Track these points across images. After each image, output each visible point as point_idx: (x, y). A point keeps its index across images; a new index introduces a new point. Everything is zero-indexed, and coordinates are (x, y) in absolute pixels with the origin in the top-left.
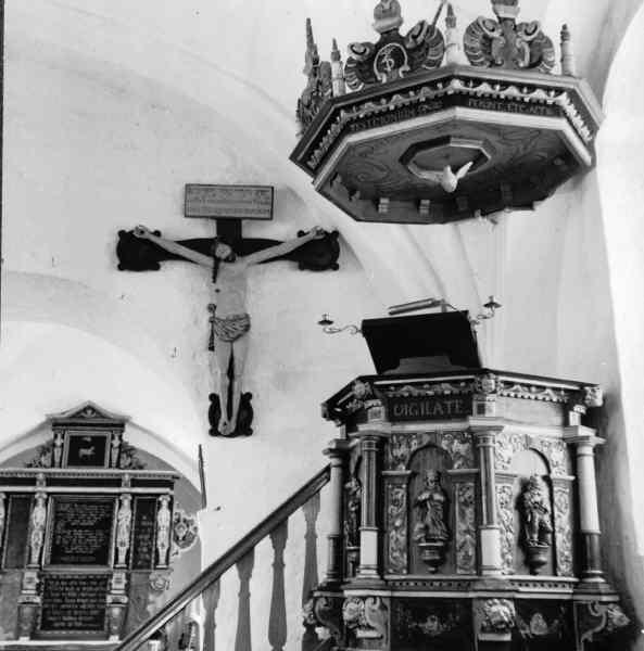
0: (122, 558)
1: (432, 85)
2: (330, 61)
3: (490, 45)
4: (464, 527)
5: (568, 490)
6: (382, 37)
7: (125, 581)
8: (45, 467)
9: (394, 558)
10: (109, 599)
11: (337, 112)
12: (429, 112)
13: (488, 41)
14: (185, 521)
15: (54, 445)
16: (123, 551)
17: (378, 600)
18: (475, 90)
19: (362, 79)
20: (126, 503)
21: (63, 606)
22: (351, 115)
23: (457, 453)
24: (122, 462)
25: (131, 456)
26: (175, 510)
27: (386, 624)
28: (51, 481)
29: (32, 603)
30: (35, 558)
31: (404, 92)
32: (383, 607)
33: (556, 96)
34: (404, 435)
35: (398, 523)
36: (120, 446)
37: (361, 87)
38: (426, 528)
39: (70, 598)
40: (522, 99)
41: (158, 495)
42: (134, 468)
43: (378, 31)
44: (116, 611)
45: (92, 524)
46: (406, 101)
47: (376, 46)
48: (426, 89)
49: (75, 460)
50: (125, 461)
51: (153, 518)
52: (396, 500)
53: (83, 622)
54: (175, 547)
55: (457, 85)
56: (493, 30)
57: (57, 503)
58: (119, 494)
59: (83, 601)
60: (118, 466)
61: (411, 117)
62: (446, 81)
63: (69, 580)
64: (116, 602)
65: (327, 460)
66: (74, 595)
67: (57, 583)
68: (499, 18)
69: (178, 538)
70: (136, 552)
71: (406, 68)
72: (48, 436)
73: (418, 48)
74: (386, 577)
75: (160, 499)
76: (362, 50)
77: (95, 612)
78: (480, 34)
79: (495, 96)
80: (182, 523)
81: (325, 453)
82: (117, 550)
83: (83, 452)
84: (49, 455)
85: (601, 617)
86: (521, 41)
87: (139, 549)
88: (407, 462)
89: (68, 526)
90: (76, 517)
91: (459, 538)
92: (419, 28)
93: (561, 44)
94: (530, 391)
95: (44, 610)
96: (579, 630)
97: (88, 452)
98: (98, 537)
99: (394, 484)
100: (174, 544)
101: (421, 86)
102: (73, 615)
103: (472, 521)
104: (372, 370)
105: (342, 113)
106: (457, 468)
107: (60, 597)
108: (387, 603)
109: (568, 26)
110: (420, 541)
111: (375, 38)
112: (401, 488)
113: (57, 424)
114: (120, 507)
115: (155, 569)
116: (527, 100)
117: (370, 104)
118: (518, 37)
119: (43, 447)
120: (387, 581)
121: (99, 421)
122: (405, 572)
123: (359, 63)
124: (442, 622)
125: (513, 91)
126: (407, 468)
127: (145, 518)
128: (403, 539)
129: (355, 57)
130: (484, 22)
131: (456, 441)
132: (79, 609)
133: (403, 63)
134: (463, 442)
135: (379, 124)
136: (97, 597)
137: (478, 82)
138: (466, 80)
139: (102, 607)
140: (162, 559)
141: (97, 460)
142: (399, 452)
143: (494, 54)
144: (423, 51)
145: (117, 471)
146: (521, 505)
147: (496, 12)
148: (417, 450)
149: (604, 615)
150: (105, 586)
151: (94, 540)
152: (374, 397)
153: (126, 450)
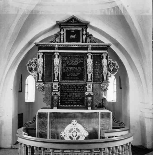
0: (89, 78)
7: (92, 87)
8: (57, 42)
10: (86, 93)
14: (113, 63)
15: (60, 34)
16: (89, 75)
20: (90, 56)
21: (68, 96)
24: (87, 40)
25: (91, 38)
26: (108, 59)
28: (60, 48)
29: (57, 95)
30: (56, 78)
36: (86, 34)
39: (71, 93)
41: (102, 53)
42: (92, 43)
44: (90, 98)
45: (76, 65)
49: (69, 40)
50: (89, 40)
51: (101, 63)
53: (76, 102)
54: (110, 74)
57: (62, 57)
58: (87, 53)
59: (76, 94)
60: (86, 42)
63: (70, 86)
64: (89, 95)
66: (72, 92)
67: (65, 87)
69: (110, 70)
70: (94, 76)
72: (57, 30)
75: (103, 55)
77: (81, 98)
80: (111, 64)
82: (87, 75)
83: (72, 36)
84: (59, 38)
87: (95, 74)
89: (67, 66)
90: (70, 63)
95: (61, 97)
97: (74, 37)
98: (79, 70)
100: (109, 73)
102: (72, 99)
107: (67, 92)
113: (60, 25)
114: (87, 59)
115: (102, 82)
119: (56, 35)
121: (77, 24)
127: (97, 62)
132: (74, 97)
136: (81, 93)
139: (83, 96)
140: (105, 78)
141: (78, 40)
145: (86, 44)
150: (84, 88)
151: (78, 71)
153: (89, 36)
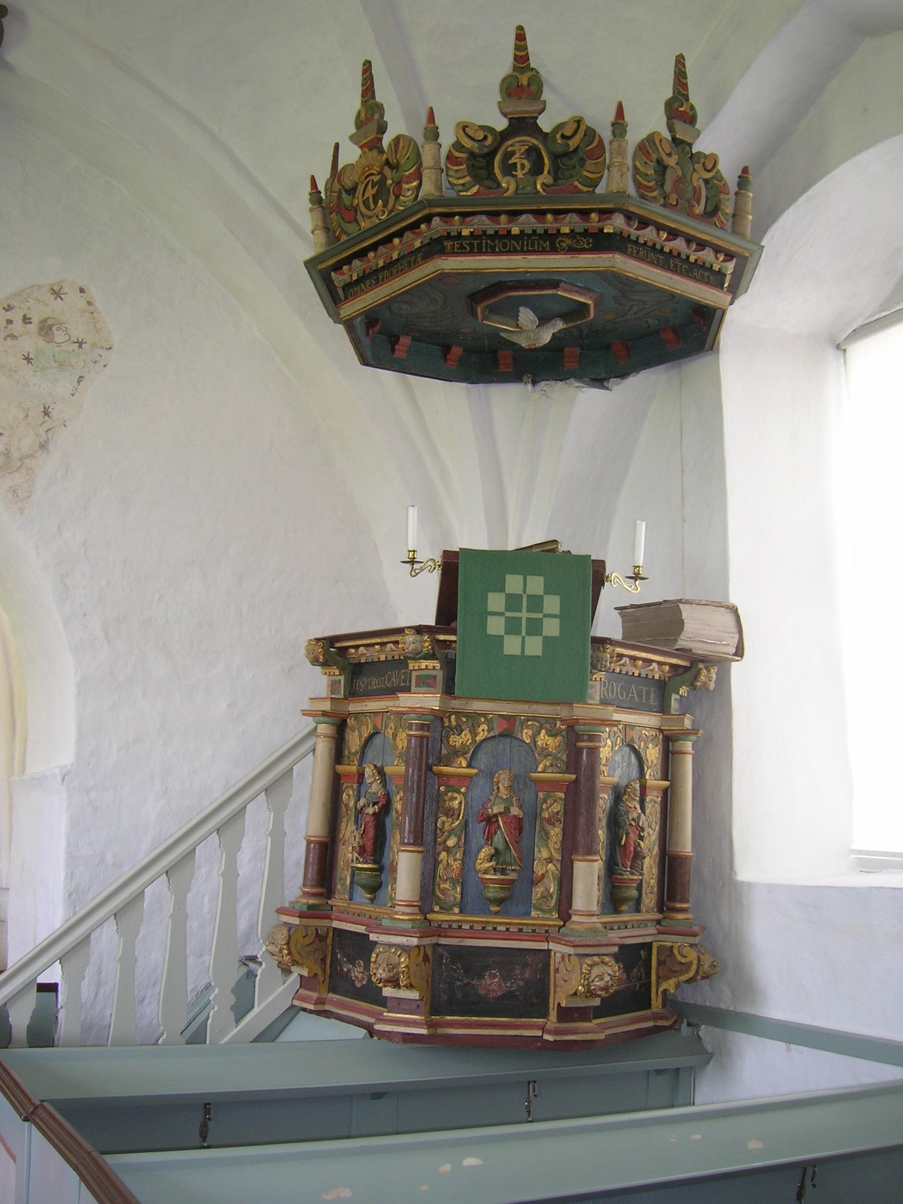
1: (584, 214)
2: (420, 140)
3: (664, 174)
4: (545, 854)
5: (660, 799)
6: (510, 123)
9: (443, 891)
11: (428, 219)
12: (571, 250)
13: (662, 168)
17: (422, 949)
18: (640, 232)
19: (477, 179)
22: (448, 227)
23: (543, 749)
27: (427, 981)
31: (540, 214)
32: (426, 959)
33: (724, 261)
34: (467, 715)
35: (451, 843)
37: (475, 189)
38: (496, 855)
40: (688, 257)
43: (505, 115)
46: (540, 228)
47: (502, 133)
48: (575, 218)
52: (451, 809)
55: (617, 223)
56: (669, 155)
61: (543, 251)
62: (605, 213)
65: (309, 723)
68: (674, 139)
71: (545, 178)
73: (567, 154)
74: (429, 916)
76: (480, 135)
78: (654, 156)
79: (658, 247)
81: (305, 713)
85: (690, 963)
86: (697, 179)
88: (469, 755)
91: (539, 869)
92: (575, 125)
93: (736, 194)
94: (635, 666)
96: (658, 977)
99: (447, 786)
101: (566, 212)
103: (558, 846)
104: (431, 621)
105: (436, 221)
106: (544, 771)
108: (429, 952)
109: (750, 169)
110: (486, 872)
111: (501, 124)
112: (459, 792)
116: (692, 259)
117: (484, 218)
118: (695, 170)
120: (430, 921)
122: (457, 910)
123: (472, 155)
124: (505, 979)
125: (679, 244)
126: (469, 766)
128: (456, 865)
129: (468, 143)
130: (661, 140)
131: (543, 731)
133: (542, 173)
134: (554, 736)
135: (493, 252)
137: (644, 223)
138: (629, 216)
142: (457, 740)
143: (668, 187)
144: (575, 160)
146: (615, 822)
147: (671, 128)
148: (486, 740)
149: (695, 962)
152: (431, 656)
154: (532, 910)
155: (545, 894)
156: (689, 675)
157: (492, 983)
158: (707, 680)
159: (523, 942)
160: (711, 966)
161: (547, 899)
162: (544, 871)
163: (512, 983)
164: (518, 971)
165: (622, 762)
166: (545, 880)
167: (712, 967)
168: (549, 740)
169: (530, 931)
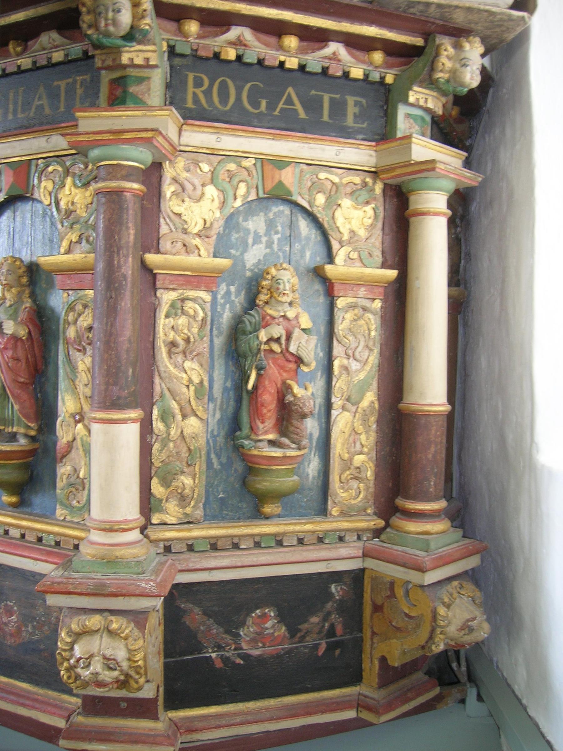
5: (378, 304)
131: (69, 180)
154: (58, 506)
155: (72, 480)
156: (419, 63)
157: (9, 621)
158: (458, 66)
159: (38, 562)
160: (462, 629)
161: (77, 489)
162: (70, 438)
163: (34, 627)
164: (41, 610)
165: (267, 233)
166: (73, 454)
167: (467, 631)
168: (76, 194)
169: (53, 543)
